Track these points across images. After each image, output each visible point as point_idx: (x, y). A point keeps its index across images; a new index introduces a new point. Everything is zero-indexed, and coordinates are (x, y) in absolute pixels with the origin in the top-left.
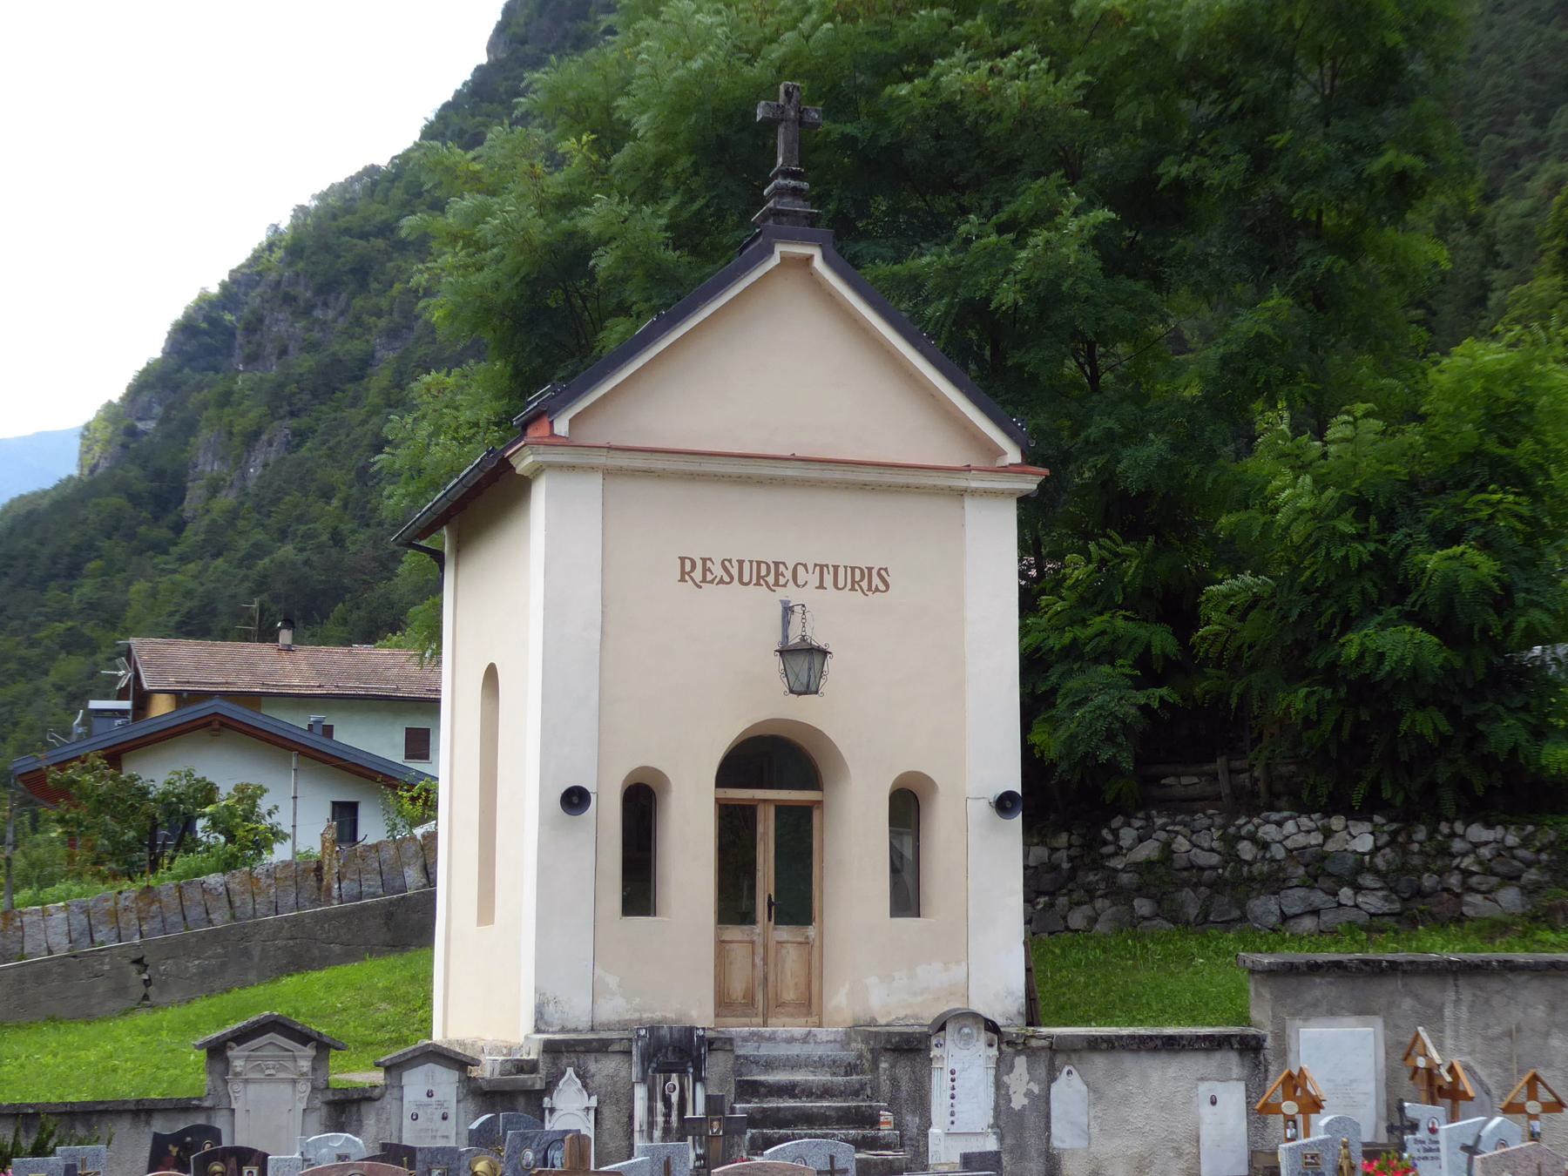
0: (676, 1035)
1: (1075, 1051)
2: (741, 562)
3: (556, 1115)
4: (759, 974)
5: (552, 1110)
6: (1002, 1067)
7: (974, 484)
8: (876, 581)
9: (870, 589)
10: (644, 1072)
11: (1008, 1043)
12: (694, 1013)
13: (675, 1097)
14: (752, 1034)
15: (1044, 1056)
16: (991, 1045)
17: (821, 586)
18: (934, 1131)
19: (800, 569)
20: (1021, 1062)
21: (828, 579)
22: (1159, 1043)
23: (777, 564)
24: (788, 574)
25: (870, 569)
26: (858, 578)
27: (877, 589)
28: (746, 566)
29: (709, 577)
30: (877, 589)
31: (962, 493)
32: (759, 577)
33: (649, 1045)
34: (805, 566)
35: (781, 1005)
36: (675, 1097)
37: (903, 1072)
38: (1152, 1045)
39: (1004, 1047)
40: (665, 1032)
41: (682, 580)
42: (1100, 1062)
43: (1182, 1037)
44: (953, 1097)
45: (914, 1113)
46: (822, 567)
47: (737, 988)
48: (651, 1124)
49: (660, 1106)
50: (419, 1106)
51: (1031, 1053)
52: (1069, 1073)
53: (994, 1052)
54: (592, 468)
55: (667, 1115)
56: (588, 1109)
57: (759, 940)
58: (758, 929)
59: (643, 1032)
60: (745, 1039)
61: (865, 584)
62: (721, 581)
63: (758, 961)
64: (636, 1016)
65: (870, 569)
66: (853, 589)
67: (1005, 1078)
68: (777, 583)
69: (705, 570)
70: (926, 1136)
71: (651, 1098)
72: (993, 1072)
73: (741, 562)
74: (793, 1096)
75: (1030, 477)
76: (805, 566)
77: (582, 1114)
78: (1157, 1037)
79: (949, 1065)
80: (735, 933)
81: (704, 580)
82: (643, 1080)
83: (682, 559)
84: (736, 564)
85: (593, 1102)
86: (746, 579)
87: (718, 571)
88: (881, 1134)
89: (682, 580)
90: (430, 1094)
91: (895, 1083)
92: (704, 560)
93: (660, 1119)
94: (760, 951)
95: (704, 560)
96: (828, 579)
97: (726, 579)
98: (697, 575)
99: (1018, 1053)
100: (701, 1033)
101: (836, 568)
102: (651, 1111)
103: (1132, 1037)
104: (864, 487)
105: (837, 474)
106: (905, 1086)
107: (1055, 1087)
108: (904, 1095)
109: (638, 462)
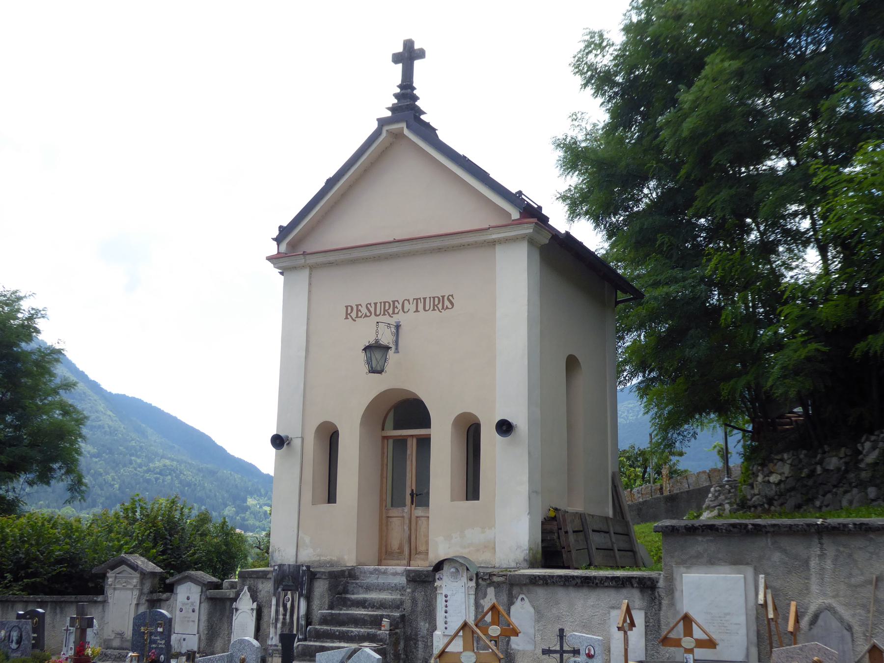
0: (291, 570)
1: (525, 585)
2: (376, 304)
3: (239, 612)
4: (407, 535)
5: (237, 610)
6: (479, 593)
7: (494, 236)
8: (447, 303)
9: (443, 308)
10: (276, 589)
11: (484, 580)
12: (346, 557)
13: (289, 605)
14: (375, 570)
15: (505, 588)
16: (471, 580)
17: (417, 311)
18: (437, 633)
19: (406, 302)
20: (491, 591)
21: (421, 306)
22: (579, 581)
23: (394, 302)
24: (400, 307)
25: (443, 297)
26: (436, 303)
27: (447, 308)
28: (378, 305)
29: (360, 314)
30: (447, 308)
31: (493, 243)
32: (385, 310)
33: (278, 575)
34: (408, 301)
35: (420, 553)
36: (289, 605)
37: (420, 595)
38: (574, 582)
39: (480, 581)
40: (286, 568)
41: (347, 318)
42: (541, 593)
43: (595, 578)
44: (446, 612)
45: (425, 620)
46: (417, 299)
47: (395, 544)
48: (277, 620)
49: (281, 609)
50: (184, 604)
51: (497, 586)
52: (522, 599)
53: (473, 584)
54: (303, 267)
55: (285, 615)
56: (252, 609)
57: (406, 516)
58: (406, 509)
59: (276, 568)
60: (371, 573)
61: (440, 306)
62: (366, 316)
63: (406, 528)
64: (318, 558)
65: (443, 297)
66: (434, 310)
67: (482, 601)
68: (394, 313)
69: (358, 310)
70: (432, 636)
71: (277, 605)
72: (472, 597)
73: (376, 304)
74: (364, 607)
75: (526, 226)
76: (408, 301)
77: (250, 612)
78: (577, 577)
79: (444, 591)
80: (395, 512)
81: (357, 317)
82: (274, 595)
83: (347, 307)
84: (373, 305)
85: (255, 606)
86: (378, 313)
87: (364, 310)
88: (379, 632)
89: (347, 318)
90: (188, 598)
91: (414, 601)
92: (357, 306)
93: (281, 617)
94: (407, 521)
95: (357, 306)
96: (421, 306)
97: (368, 314)
98: (354, 315)
99: (489, 585)
100: (304, 568)
101: (425, 299)
102: (277, 612)
103: (560, 577)
104: (439, 250)
105: (419, 246)
106: (420, 605)
107: (513, 609)
108: (419, 609)
109: (320, 259)
